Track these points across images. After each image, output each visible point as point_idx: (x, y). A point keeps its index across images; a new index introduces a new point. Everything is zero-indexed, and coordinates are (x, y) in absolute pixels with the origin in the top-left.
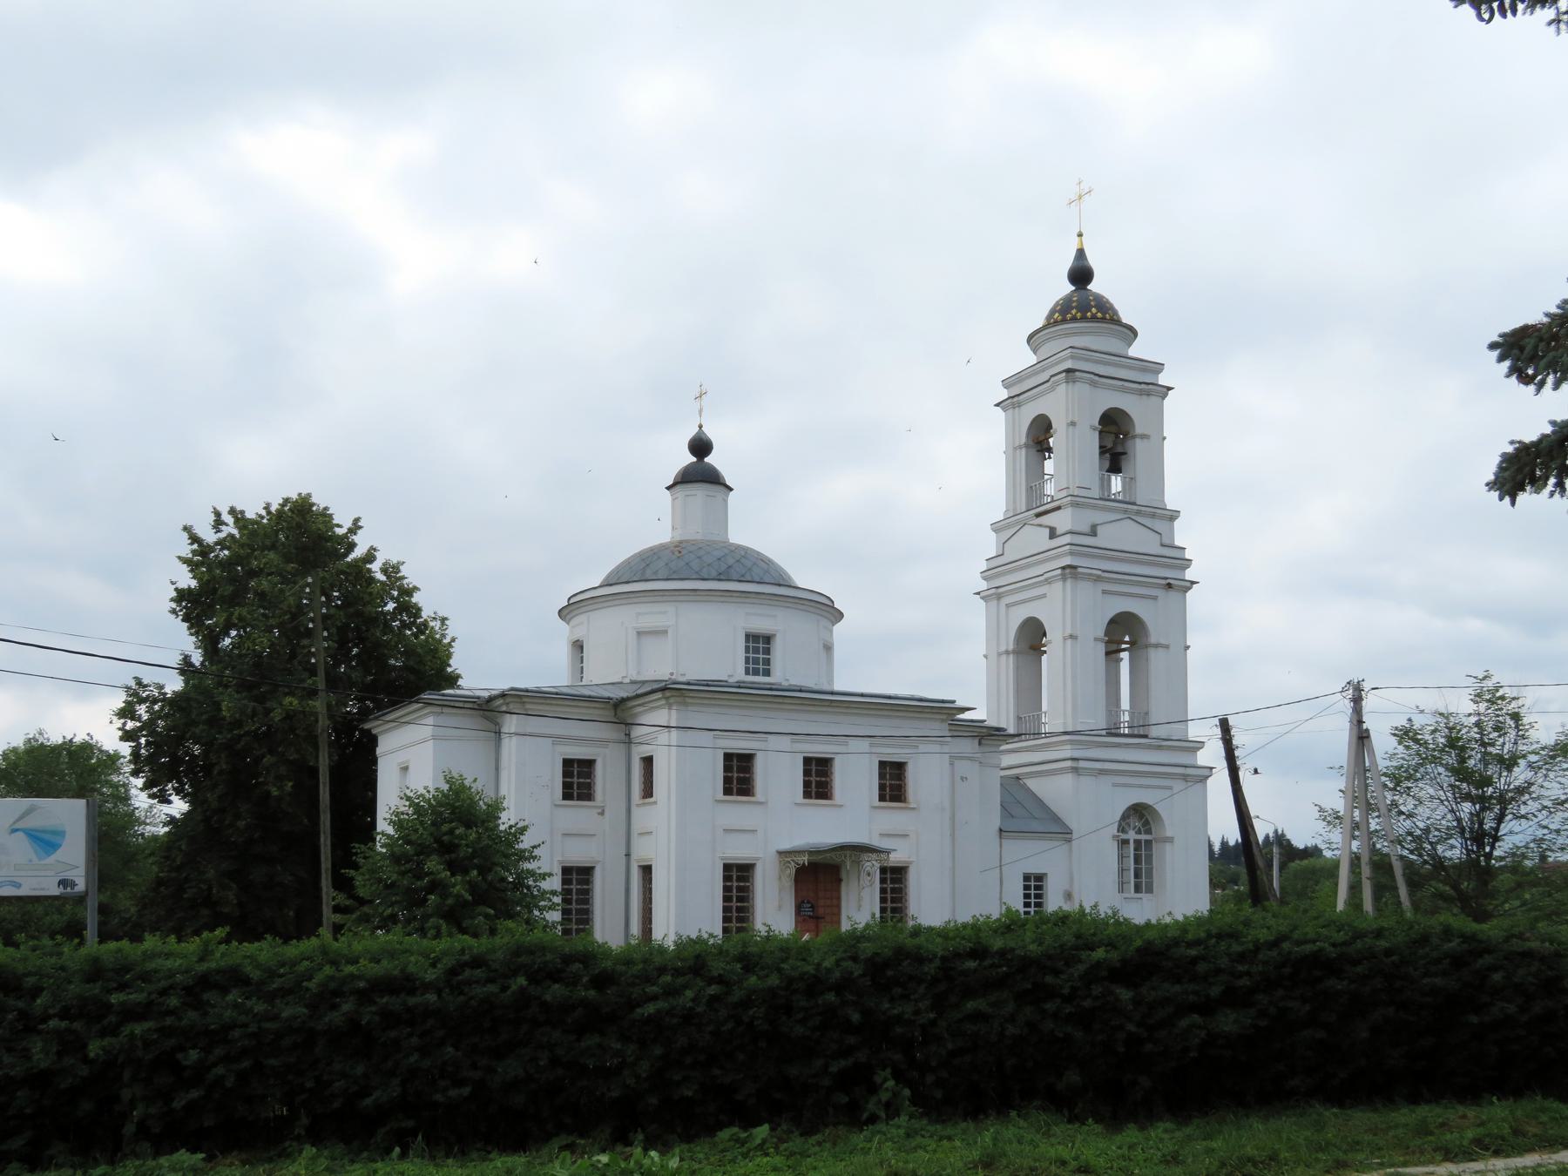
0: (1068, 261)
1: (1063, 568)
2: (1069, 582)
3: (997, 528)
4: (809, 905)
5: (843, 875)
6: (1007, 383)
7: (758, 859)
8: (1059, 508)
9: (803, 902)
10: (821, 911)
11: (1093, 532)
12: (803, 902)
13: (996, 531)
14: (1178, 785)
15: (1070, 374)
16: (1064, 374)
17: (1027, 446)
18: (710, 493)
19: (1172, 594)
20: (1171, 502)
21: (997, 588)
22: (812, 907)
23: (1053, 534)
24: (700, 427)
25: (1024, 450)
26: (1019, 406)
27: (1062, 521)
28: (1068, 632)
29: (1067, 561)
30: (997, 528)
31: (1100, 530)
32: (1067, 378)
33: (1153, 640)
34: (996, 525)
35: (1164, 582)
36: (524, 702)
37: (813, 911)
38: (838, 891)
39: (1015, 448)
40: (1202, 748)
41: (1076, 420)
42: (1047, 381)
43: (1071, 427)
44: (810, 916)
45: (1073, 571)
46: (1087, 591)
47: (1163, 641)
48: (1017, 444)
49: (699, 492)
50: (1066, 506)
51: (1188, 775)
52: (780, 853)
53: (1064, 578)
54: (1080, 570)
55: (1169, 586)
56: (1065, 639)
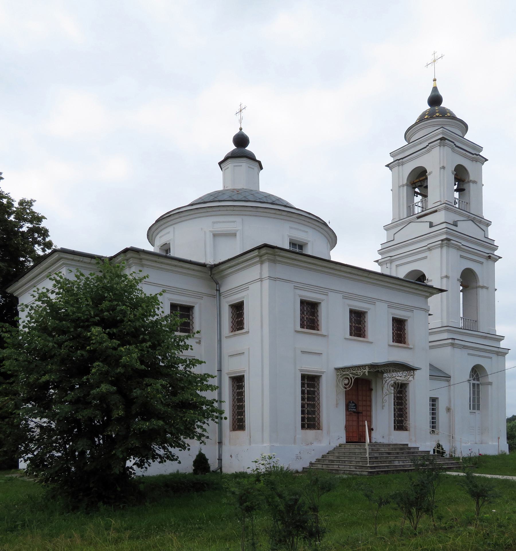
0: (428, 94)
1: (442, 240)
2: (445, 249)
3: (387, 228)
4: (354, 405)
5: (373, 386)
6: (392, 154)
7: (323, 372)
8: (436, 211)
9: (350, 402)
10: (360, 409)
11: (455, 224)
12: (350, 402)
13: (386, 230)
14: (494, 357)
15: (443, 141)
16: (439, 141)
17: (407, 185)
18: (251, 166)
19: (490, 262)
20: (487, 215)
21: (391, 257)
22: (355, 405)
23: (431, 225)
24: (241, 129)
25: (405, 187)
26: (402, 165)
27: (438, 218)
28: (444, 274)
29: (444, 237)
30: (387, 228)
31: (459, 223)
32: (440, 143)
33: (481, 284)
34: (386, 227)
35: (487, 255)
36: (141, 259)
37: (356, 408)
38: (370, 396)
39: (400, 187)
40: (503, 339)
41: (445, 165)
42: (425, 147)
43: (442, 169)
44: (354, 412)
45: (448, 242)
46: (454, 254)
47: (485, 285)
48: (401, 184)
49: (244, 164)
50: (440, 210)
51: (499, 352)
52: (337, 369)
53: (441, 246)
54: (452, 242)
55: (489, 257)
56: (442, 278)
